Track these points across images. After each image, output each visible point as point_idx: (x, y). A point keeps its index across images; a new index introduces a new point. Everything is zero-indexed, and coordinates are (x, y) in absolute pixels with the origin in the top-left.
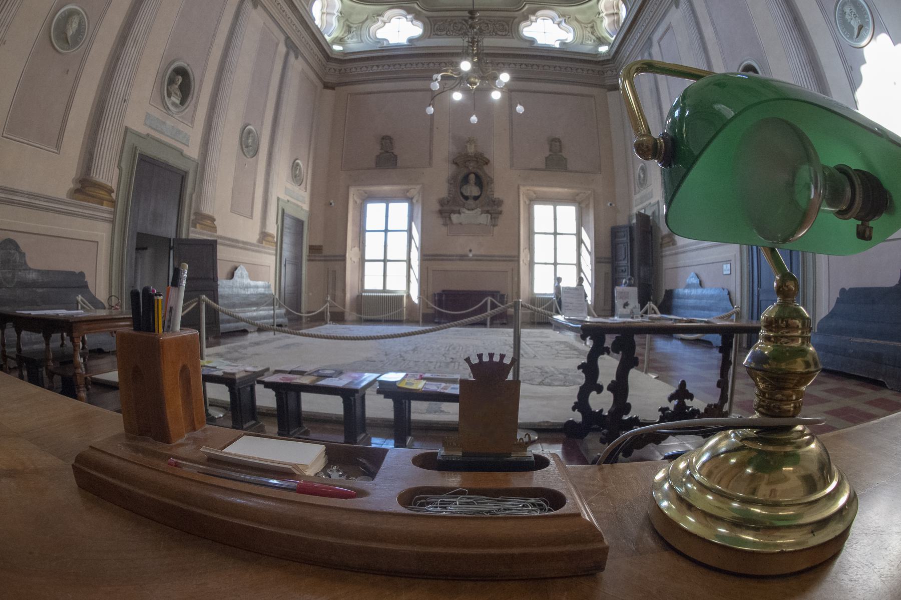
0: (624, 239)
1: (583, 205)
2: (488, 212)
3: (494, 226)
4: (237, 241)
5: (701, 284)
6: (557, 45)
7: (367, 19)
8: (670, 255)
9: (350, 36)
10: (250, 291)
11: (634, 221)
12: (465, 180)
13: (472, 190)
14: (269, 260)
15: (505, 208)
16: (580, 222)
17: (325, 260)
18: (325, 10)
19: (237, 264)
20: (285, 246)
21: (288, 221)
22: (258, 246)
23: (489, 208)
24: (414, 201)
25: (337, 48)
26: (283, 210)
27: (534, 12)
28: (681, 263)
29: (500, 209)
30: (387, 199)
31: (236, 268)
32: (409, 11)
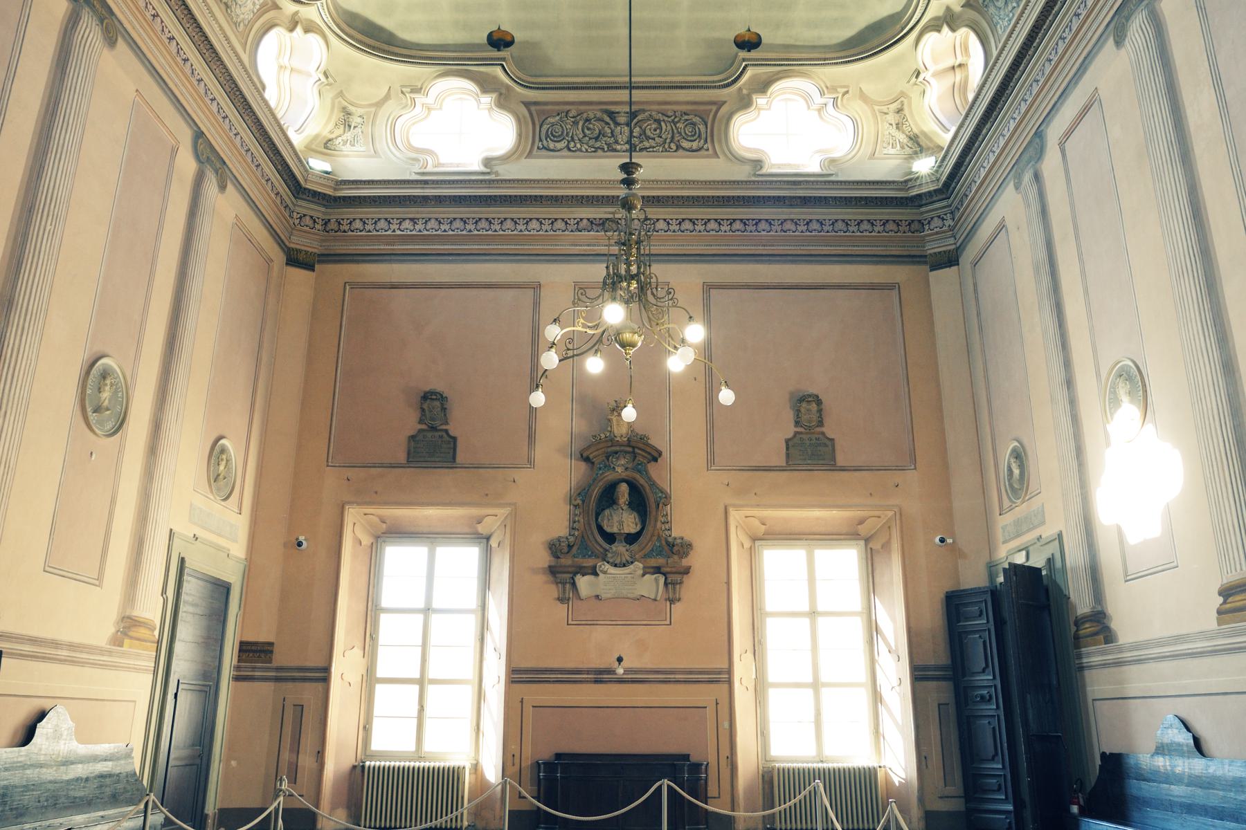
0: (981, 623)
1: (876, 545)
2: (657, 570)
3: (672, 601)
4: (55, 644)
5: (1198, 746)
7: (387, 97)
8: (1105, 665)
9: (348, 135)
10: (80, 771)
11: (1001, 579)
12: (608, 497)
13: (624, 520)
14: (132, 687)
15: (696, 560)
17: (277, 679)
18: (285, 61)
19: (46, 704)
20: (179, 647)
21: (192, 587)
22: (110, 653)
23: (660, 561)
24: (494, 543)
25: (318, 165)
26: (182, 561)
27: (763, 86)
28: (1133, 689)
29: (685, 562)
31: (42, 715)
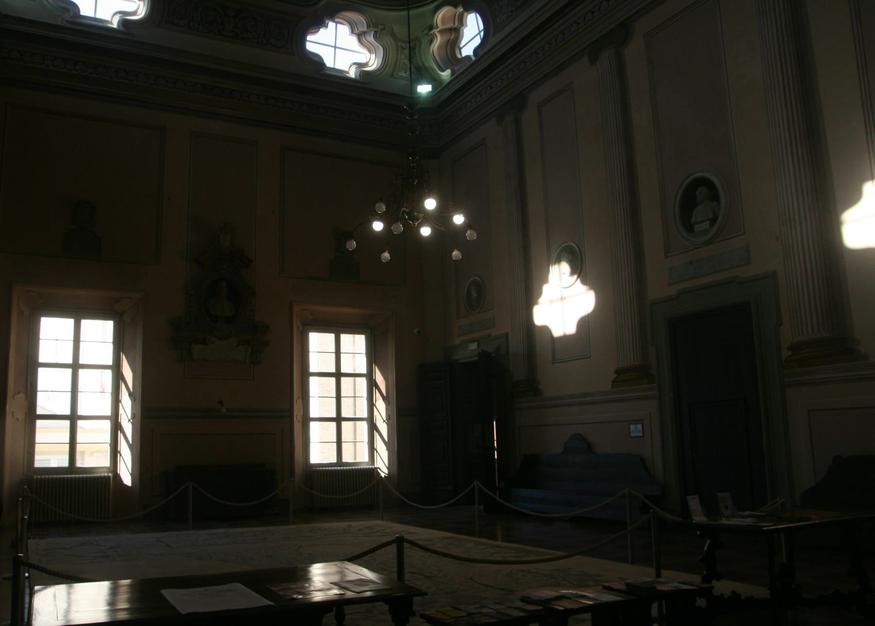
6: (352, 74)
16: (374, 356)
30: (78, 311)
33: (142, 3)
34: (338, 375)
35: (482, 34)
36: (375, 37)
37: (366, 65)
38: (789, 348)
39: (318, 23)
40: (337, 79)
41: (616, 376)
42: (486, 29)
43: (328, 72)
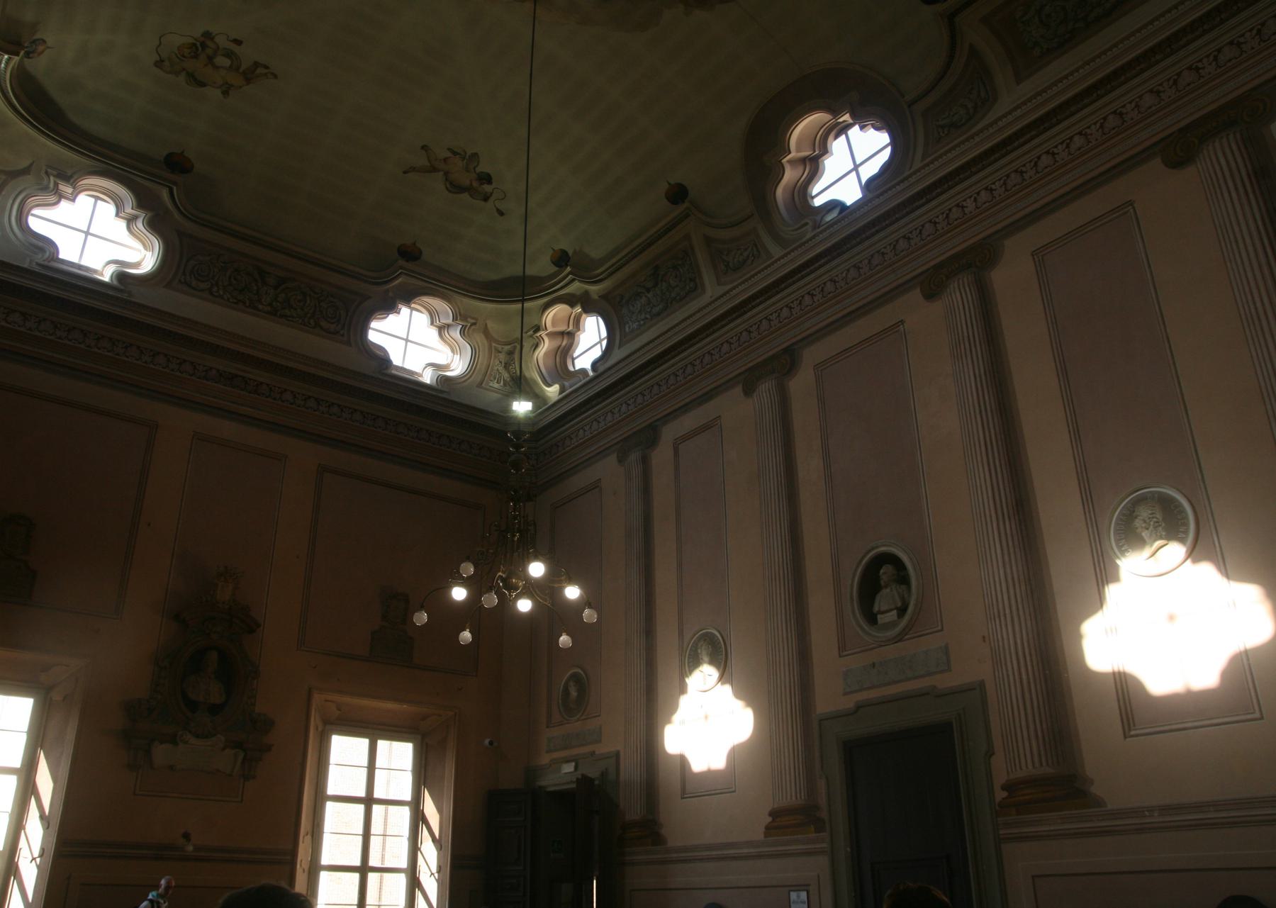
6: (427, 378)
16: (423, 775)
32: (145, 201)
33: (149, 254)
34: (369, 801)
35: (604, 343)
36: (462, 333)
37: (446, 367)
38: (1004, 788)
39: (388, 307)
40: (406, 386)
41: (770, 819)
42: (610, 337)
43: (394, 372)
